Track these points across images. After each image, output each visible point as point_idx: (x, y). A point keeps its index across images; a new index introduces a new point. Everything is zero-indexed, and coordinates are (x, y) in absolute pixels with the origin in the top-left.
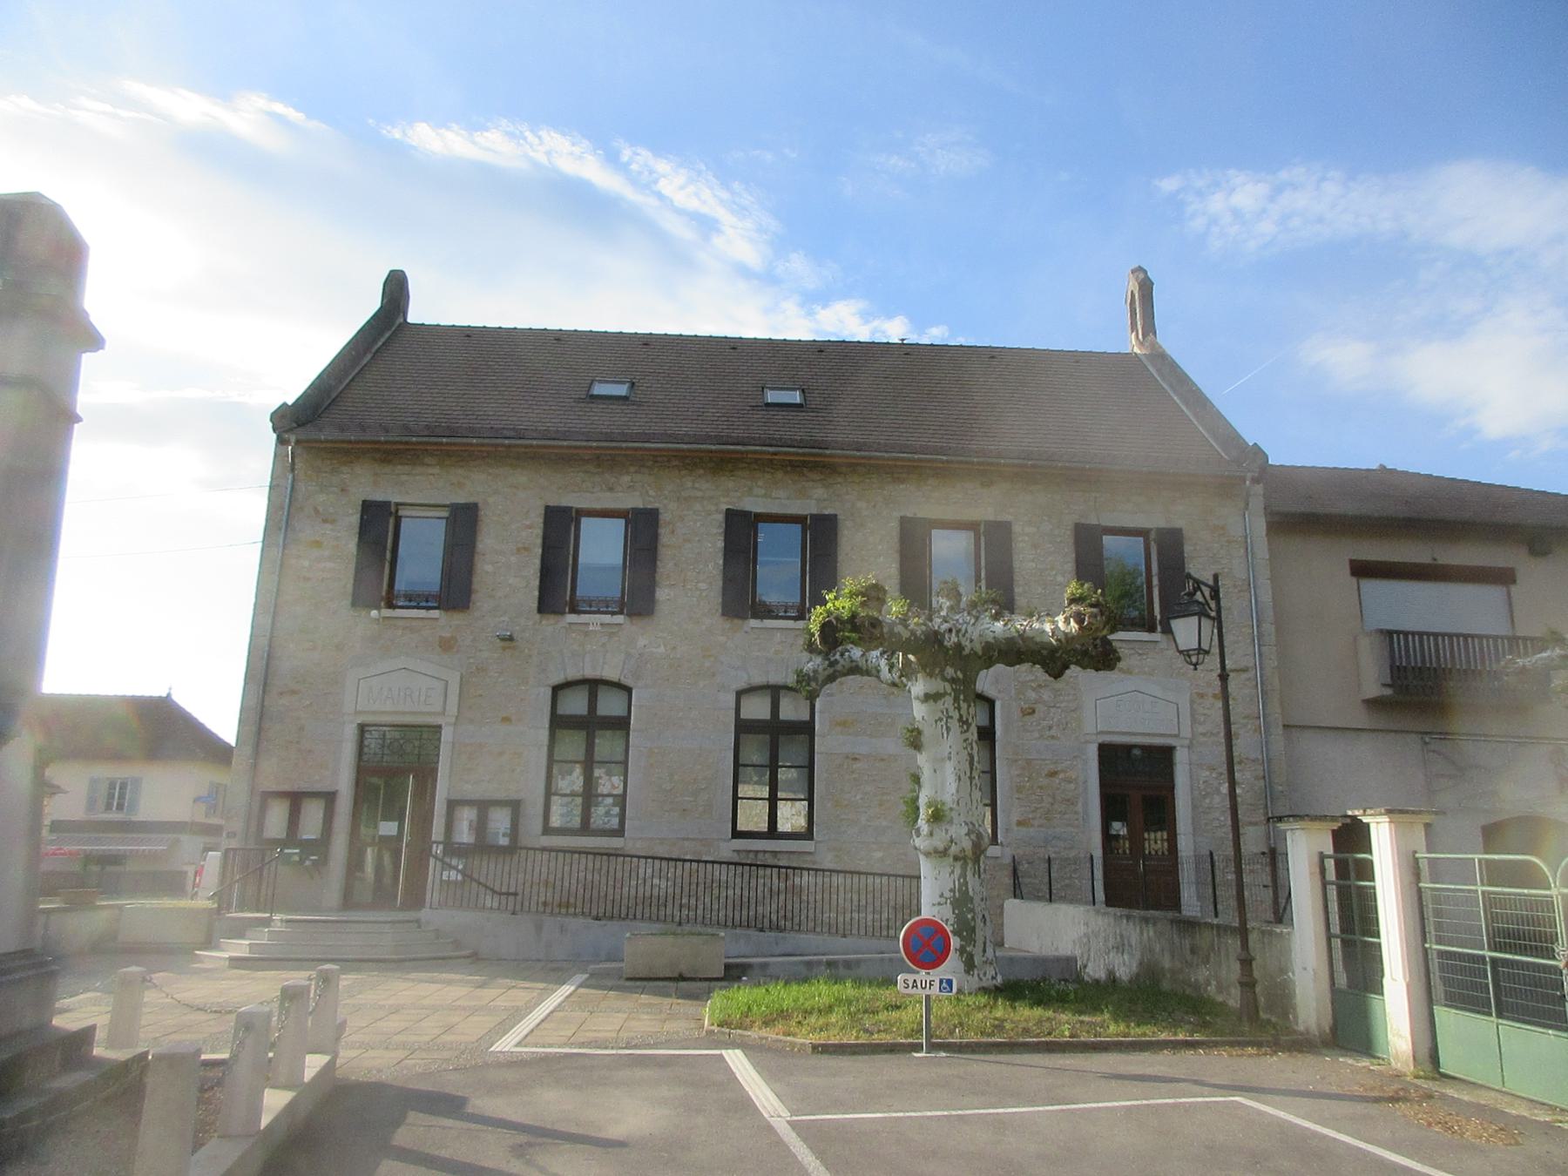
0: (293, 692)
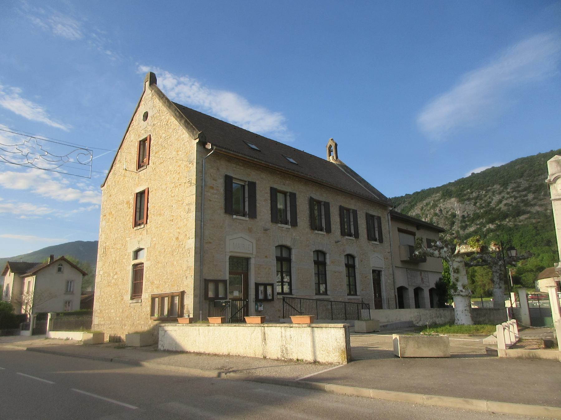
0: (210, 243)
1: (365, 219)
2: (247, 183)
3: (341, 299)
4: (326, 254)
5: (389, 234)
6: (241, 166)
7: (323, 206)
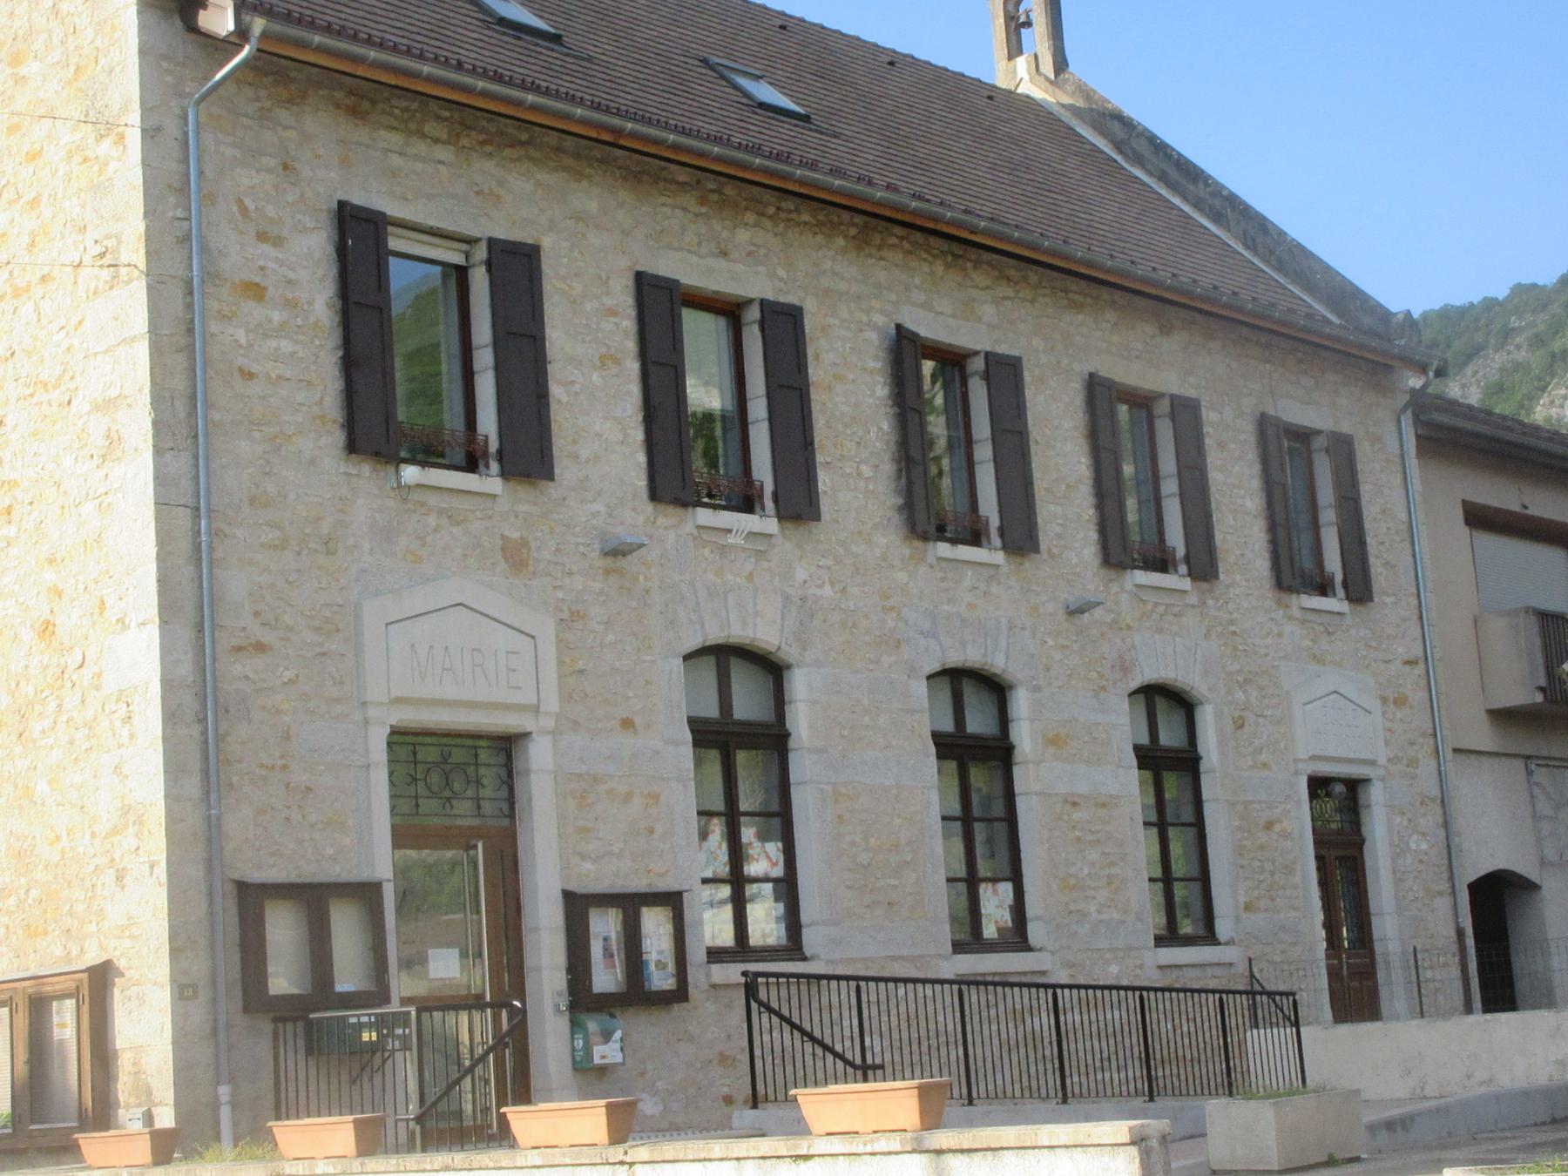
0: (261, 648)
1: (1252, 454)
2: (481, 253)
3: (1114, 969)
4: (1012, 687)
5: (1407, 544)
6: (436, 141)
7: (984, 383)
